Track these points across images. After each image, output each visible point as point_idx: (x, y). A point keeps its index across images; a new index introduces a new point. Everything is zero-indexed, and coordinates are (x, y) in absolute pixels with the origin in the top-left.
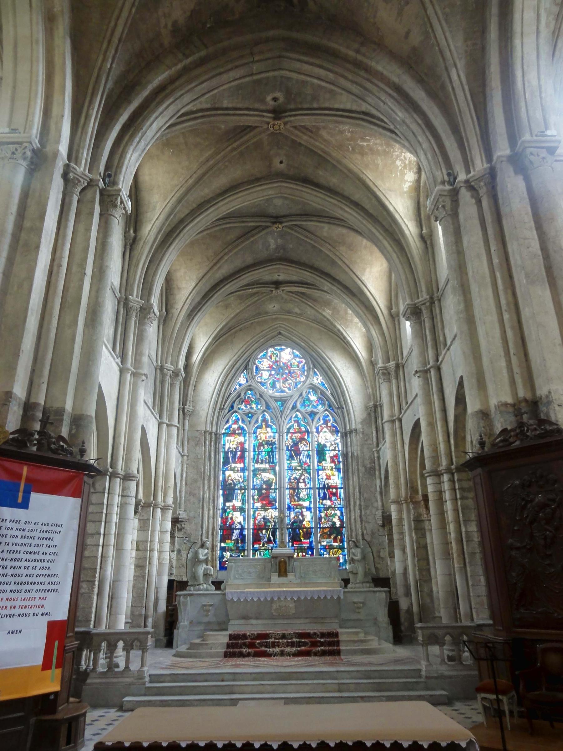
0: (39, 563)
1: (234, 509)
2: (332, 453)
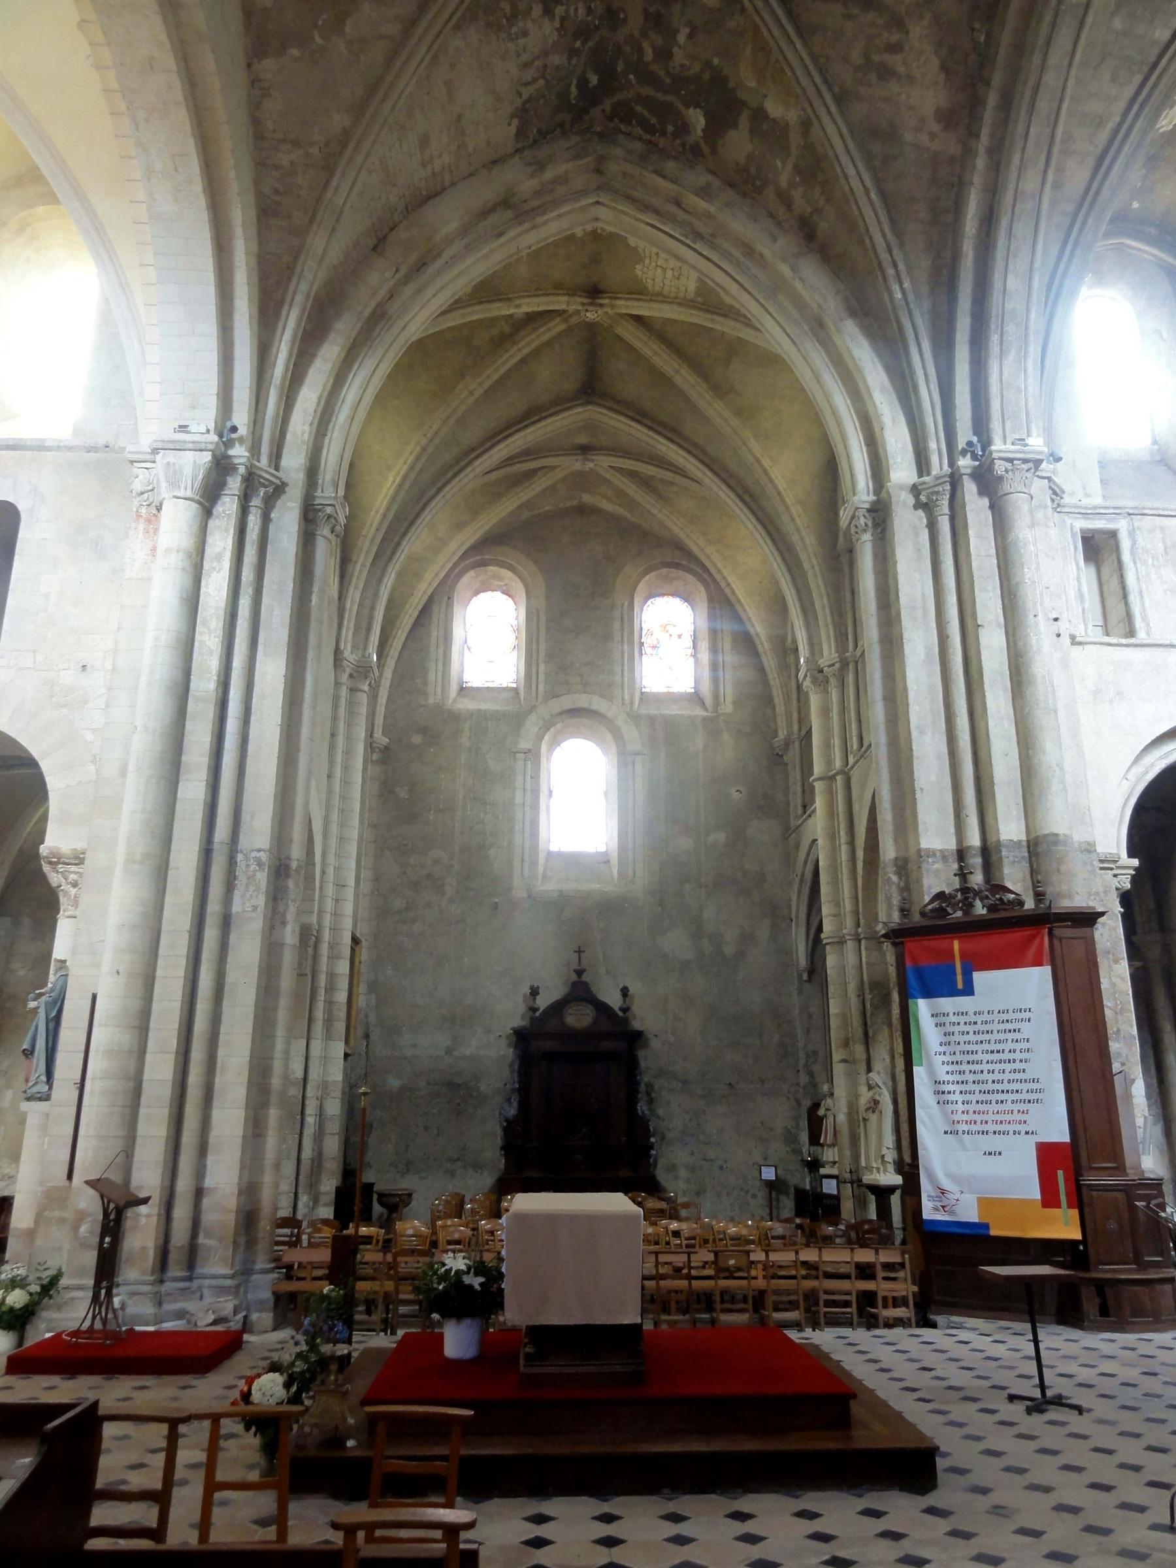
0: (1007, 1065)
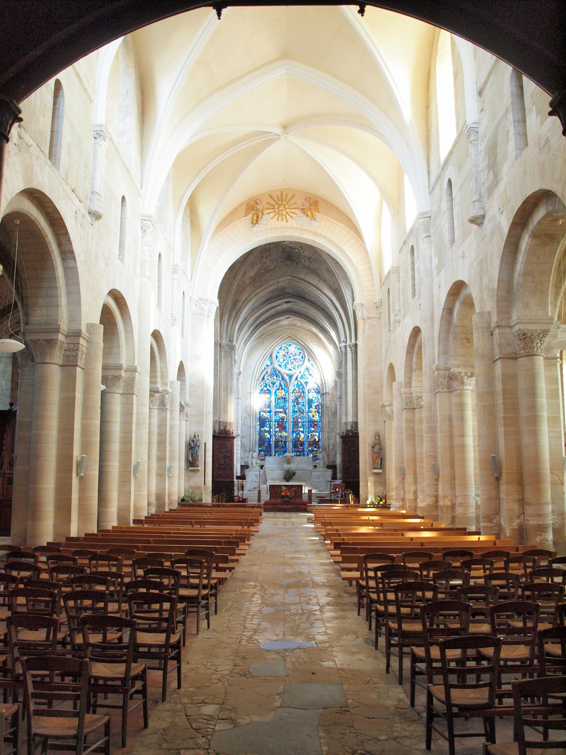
1: (266, 431)
2: (316, 404)
